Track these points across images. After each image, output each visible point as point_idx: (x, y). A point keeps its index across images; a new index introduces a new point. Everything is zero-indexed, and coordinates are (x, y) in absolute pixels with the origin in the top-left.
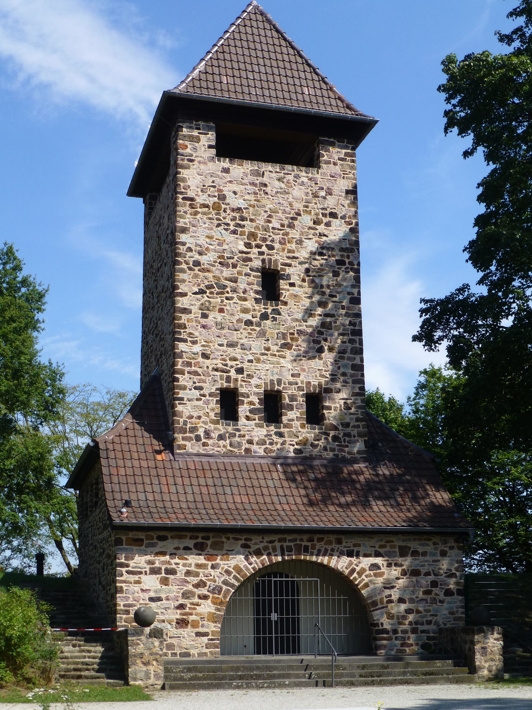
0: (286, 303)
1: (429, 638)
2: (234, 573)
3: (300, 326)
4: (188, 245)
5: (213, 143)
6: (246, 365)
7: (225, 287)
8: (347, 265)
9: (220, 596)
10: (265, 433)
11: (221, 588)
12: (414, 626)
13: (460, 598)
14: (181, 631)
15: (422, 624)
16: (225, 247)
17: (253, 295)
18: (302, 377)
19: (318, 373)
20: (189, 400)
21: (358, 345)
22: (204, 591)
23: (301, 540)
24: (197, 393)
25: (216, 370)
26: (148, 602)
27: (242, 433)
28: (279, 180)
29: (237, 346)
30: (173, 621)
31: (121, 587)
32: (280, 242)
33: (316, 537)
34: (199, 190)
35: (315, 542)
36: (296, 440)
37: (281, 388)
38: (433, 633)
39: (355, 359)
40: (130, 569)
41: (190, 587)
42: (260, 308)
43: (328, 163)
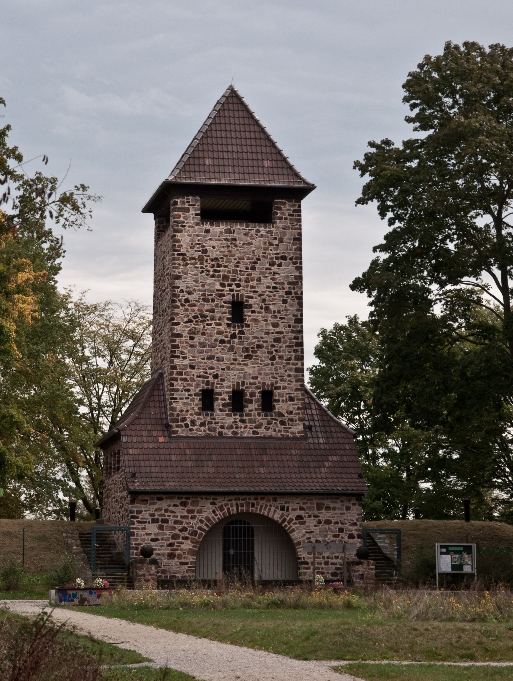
0: (248, 326)
1: (336, 569)
2: (205, 522)
3: (258, 341)
4: (181, 288)
5: (199, 212)
6: (220, 372)
7: (206, 316)
8: (293, 295)
9: (196, 538)
10: (233, 420)
11: (197, 532)
12: (326, 560)
13: (360, 540)
14: (170, 561)
15: (332, 558)
16: (206, 287)
17: (226, 321)
18: (259, 379)
19: (270, 376)
20: (181, 399)
21: (300, 354)
22: (186, 534)
23: (250, 499)
24: (187, 393)
25: (199, 376)
26: (150, 542)
27: (217, 421)
28: (246, 234)
29: (214, 359)
30: (165, 554)
31: (134, 532)
32: (246, 281)
33: (259, 497)
34: (189, 247)
35: (259, 500)
36: (254, 425)
37: (244, 388)
38: (340, 565)
39: (297, 364)
40: (139, 520)
41: (177, 532)
42: (231, 330)
43: (280, 218)
